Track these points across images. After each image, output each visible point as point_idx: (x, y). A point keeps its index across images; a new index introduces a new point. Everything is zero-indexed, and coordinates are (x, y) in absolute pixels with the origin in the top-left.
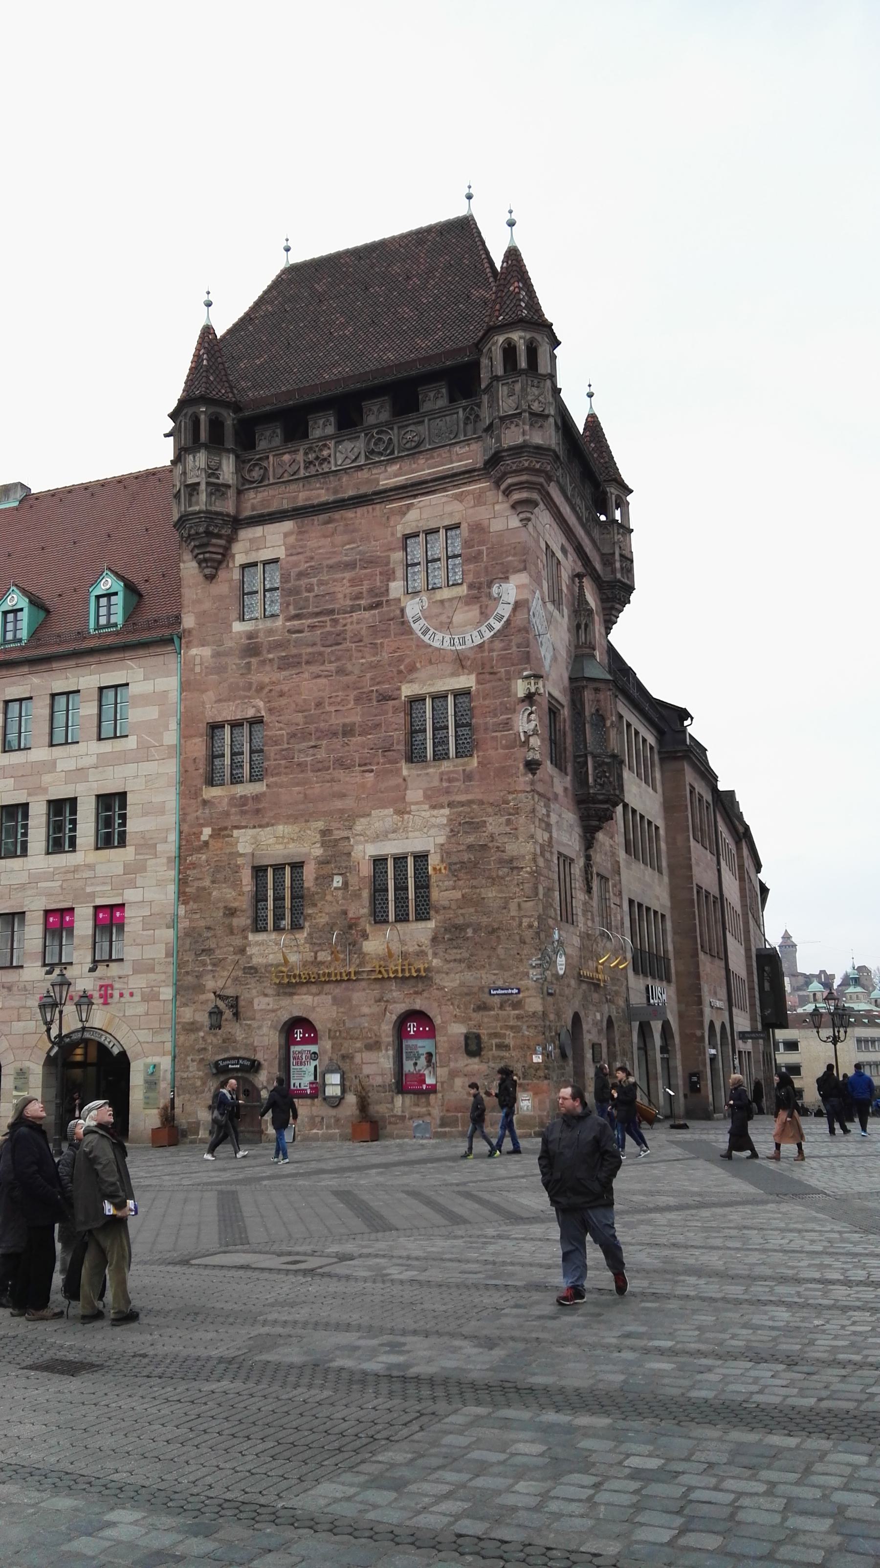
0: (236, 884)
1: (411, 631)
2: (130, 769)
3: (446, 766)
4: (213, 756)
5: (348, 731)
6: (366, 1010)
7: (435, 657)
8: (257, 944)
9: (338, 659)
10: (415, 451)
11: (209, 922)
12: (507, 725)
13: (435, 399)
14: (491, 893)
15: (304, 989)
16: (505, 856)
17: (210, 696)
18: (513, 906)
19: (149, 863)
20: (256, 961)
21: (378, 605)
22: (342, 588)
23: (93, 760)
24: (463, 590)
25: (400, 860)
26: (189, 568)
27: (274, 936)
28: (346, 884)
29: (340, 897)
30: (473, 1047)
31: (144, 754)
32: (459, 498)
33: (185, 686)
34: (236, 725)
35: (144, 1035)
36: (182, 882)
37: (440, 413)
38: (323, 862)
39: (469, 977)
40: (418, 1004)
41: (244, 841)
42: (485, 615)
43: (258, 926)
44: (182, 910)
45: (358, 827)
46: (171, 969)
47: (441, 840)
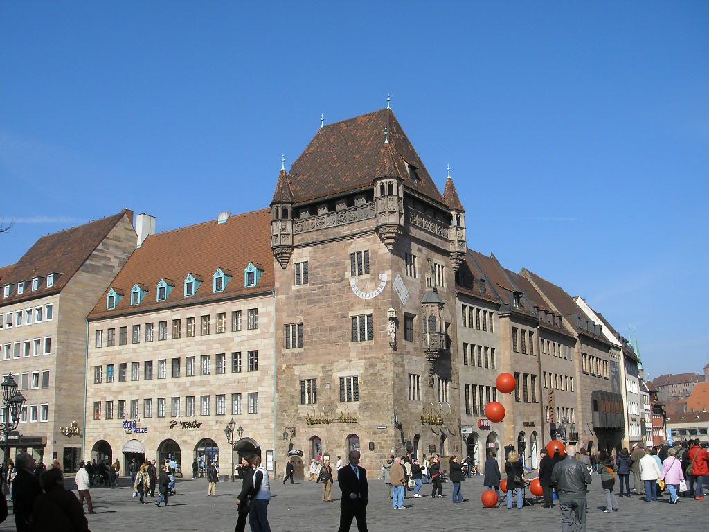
0: (294, 387)
1: (352, 291)
5: (331, 329)
6: (337, 434)
7: (359, 301)
8: (302, 409)
9: (328, 301)
10: (353, 221)
11: (286, 400)
12: (384, 328)
13: (361, 202)
14: (378, 392)
15: (317, 426)
16: (383, 378)
17: (284, 314)
18: (385, 396)
19: (266, 377)
20: (301, 415)
21: (341, 280)
22: (329, 273)
23: (245, 338)
24: (369, 276)
25: (349, 379)
26: (277, 264)
27: (307, 406)
28: (330, 387)
29: (328, 393)
30: (372, 447)
31: (263, 336)
33: (277, 310)
34: (294, 326)
35: (266, 441)
36: (277, 385)
37: (362, 207)
38: (323, 379)
39: (370, 422)
41: (297, 370)
42: (377, 286)
43: (303, 402)
44: (276, 395)
45: (334, 367)
46: (274, 417)
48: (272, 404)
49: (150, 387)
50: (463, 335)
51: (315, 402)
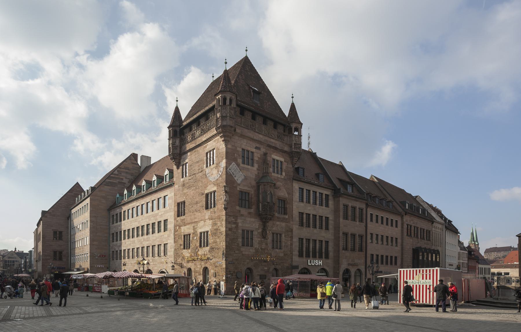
2: (168, 214)
3: (212, 210)
4: (178, 211)
5: (197, 203)
24: (215, 165)
29: (195, 242)
32: (215, 141)
36: (174, 239)
40: (207, 265)
43: (184, 248)
47: (211, 228)
48: (173, 250)
49: (129, 243)
50: (297, 207)
51: (189, 248)
